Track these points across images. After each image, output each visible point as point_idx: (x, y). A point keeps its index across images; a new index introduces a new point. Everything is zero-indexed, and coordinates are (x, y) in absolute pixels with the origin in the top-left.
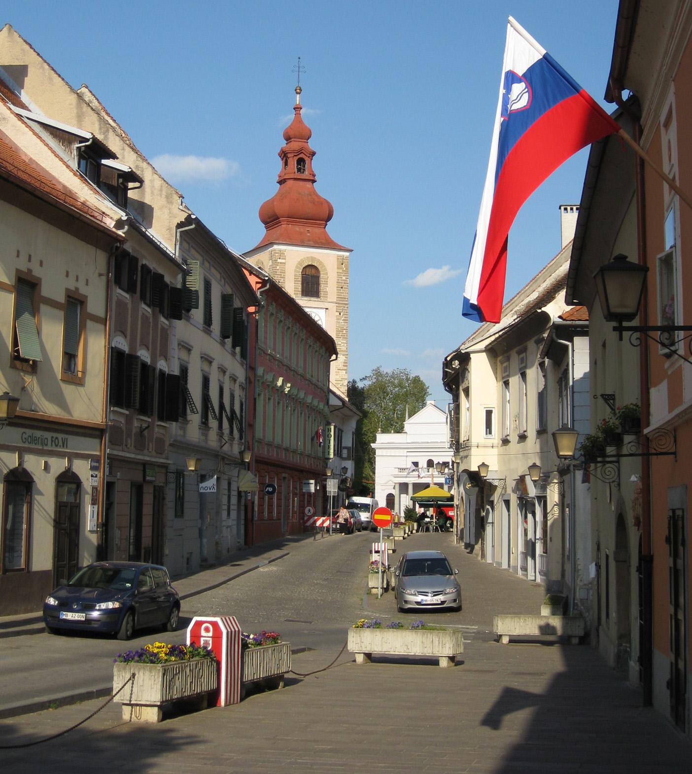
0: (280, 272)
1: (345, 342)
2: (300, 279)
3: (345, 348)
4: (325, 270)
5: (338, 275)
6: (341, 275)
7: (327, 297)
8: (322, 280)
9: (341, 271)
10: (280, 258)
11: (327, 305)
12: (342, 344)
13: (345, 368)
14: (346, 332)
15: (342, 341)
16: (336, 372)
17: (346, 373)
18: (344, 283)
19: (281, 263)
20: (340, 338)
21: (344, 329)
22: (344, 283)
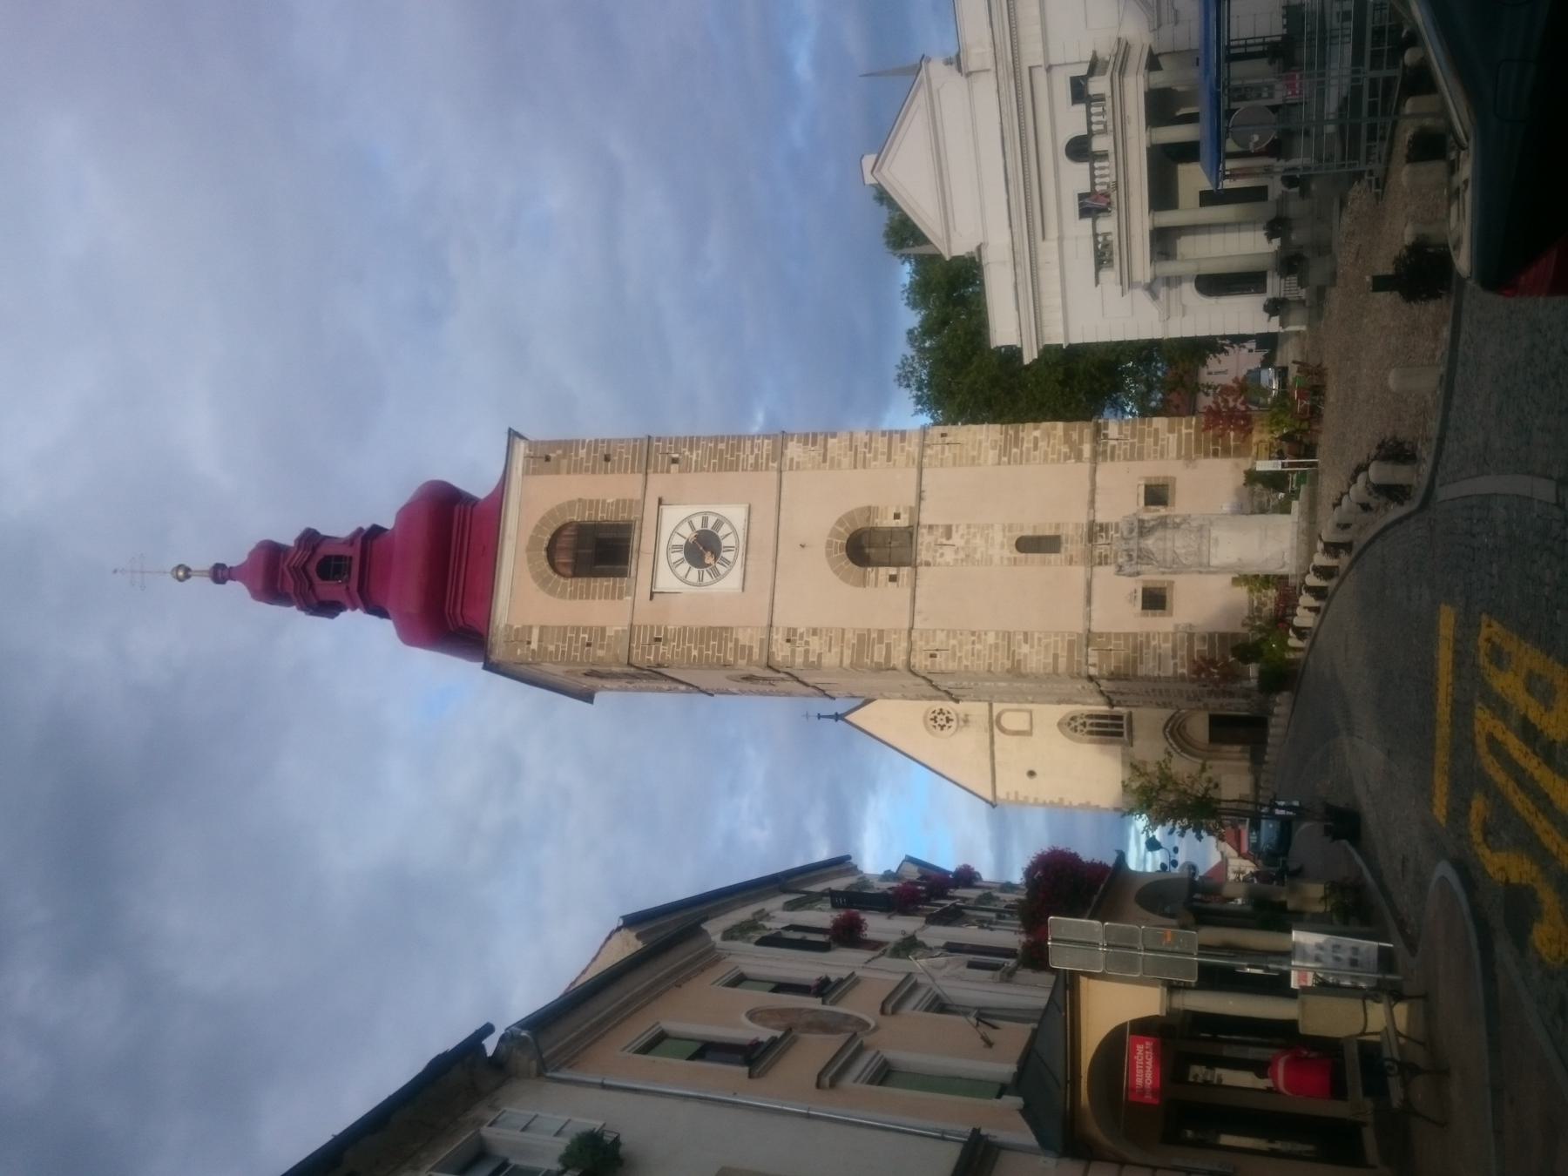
0: (564, 642)
1: (748, 444)
2: (581, 582)
3: (766, 441)
4: (560, 508)
5: (575, 471)
6: (576, 461)
7: (631, 501)
8: (586, 516)
9: (564, 462)
10: (529, 643)
11: (651, 504)
12: (756, 451)
13: (820, 439)
14: (722, 442)
15: (748, 451)
16: (832, 467)
17: (834, 435)
18: (596, 451)
19: (540, 640)
20: (738, 456)
21: (716, 445)
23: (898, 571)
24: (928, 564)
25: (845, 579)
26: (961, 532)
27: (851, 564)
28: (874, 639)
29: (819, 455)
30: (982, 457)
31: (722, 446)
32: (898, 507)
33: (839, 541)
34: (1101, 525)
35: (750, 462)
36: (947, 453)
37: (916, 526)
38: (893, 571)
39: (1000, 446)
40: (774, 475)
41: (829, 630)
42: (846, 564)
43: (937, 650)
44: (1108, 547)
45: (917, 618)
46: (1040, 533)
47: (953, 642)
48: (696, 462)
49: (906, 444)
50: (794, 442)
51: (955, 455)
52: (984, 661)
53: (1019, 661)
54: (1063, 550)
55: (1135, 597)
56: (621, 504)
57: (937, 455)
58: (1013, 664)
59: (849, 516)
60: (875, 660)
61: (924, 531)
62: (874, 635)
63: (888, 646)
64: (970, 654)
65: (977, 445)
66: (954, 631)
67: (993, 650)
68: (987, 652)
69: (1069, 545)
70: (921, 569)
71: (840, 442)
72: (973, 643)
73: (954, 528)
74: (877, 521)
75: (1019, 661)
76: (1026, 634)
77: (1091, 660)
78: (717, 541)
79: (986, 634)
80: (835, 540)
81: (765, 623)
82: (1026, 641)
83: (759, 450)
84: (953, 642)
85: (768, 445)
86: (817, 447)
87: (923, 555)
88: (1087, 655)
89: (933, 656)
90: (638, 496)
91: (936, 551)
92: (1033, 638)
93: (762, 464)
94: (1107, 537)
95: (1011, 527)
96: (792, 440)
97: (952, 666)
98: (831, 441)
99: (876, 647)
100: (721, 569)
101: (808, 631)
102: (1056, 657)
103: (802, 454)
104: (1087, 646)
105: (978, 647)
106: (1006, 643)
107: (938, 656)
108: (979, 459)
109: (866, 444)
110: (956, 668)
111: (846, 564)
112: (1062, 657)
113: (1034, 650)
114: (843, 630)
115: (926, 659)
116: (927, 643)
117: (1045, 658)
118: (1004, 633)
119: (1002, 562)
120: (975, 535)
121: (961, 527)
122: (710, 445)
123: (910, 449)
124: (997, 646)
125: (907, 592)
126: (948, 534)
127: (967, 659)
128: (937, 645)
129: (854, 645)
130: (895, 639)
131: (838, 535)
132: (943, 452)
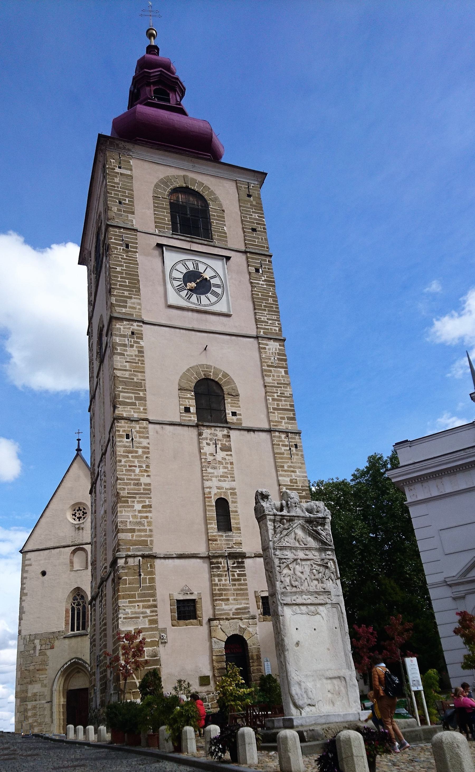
1: (274, 317)
3: (277, 329)
12: (270, 322)
14: (273, 301)
20: (265, 310)
21: (271, 297)
22: (257, 223)
23: (193, 414)
24: (200, 434)
25: (184, 376)
26: (227, 457)
27: (196, 381)
28: (139, 394)
29: (272, 363)
30: (283, 473)
31: (271, 300)
32: (240, 415)
33: (212, 374)
34: (243, 562)
35: (262, 317)
36: (283, 448)
37: (228, 426)
38: (193, 410)
39: (293, 486)
40: (254, 333)
41: (143, 362)
42: (195, 378)
43: (132, 439)
44: (226, 569)
45: (157, 427)
46: (232, 516)
47: (140, 451)
48: (258, 284)
49: (286, 421)
50: (278, 347)
51: (283, 454)
52: (125, 475)
53: (127, 502)
54: (220, 534)
55: (187, 594)
56: (224, 236)
57: (281, 441)
58: (123, 497)
59: (230, 381)
60: (121, 394)
61: (225, 432)
62: (141, 394)
63: (134, 404)
64: (131, 464)
65: (292, 469)
66: (148, 453)
67: (136, 482)
68: (133, 477)
69: (224, 538)
70: (194, 432)
71: (283, 377)
72: (140, 467)
73: (229, 453)
74: (229, 400)
75: (127, 502)
76: (150, 506)
77: (130, 560)
78: (205, 293)
79: (148, 476)
80: (212, 371)
81: (146, 319)
82: (143, 507)
83: (270, 323)
84: (140, 451)
85: (275, 330)
86: (277, 362)
87: (207, 432)
88: (135, 556)
89: (128, 437)
90: (230, 245)
91: (211, 440)
92: (146, 512)
93: (262, 325)
94: (233, 567)
95: (234, 494)
96: (280, 345)
97: (120, 451)
98: (282, 370)
99: (133, 395)
100: (184, 293)
101: (142, 347)
102: (133, 531)
103: (271, 351)
104: (143, 556)
105: (137, 470)
106: (142, 491)
107: (128, 440)
108: (282, 471)
109: (284, 394)
110: (118, 453)
111: (195, 378)
112: (133, 536)
113: (137, 514)
114: (144, 372)
115: (124, 431)
116: (137, 432)
117: (130, 522)
118: (150, 490)
119: (207, 488)
120: (225, 468)
121: (229, 457)
122: (271, 293)
123: (283, 424)
124: (138, 484)
125: (177, 420)
126: (226, 449)
127: (125, 462)
128: (137, 439)
129: (133, 379)
130: (139, 409)
131: (216, 374)
132: (286, 446)
